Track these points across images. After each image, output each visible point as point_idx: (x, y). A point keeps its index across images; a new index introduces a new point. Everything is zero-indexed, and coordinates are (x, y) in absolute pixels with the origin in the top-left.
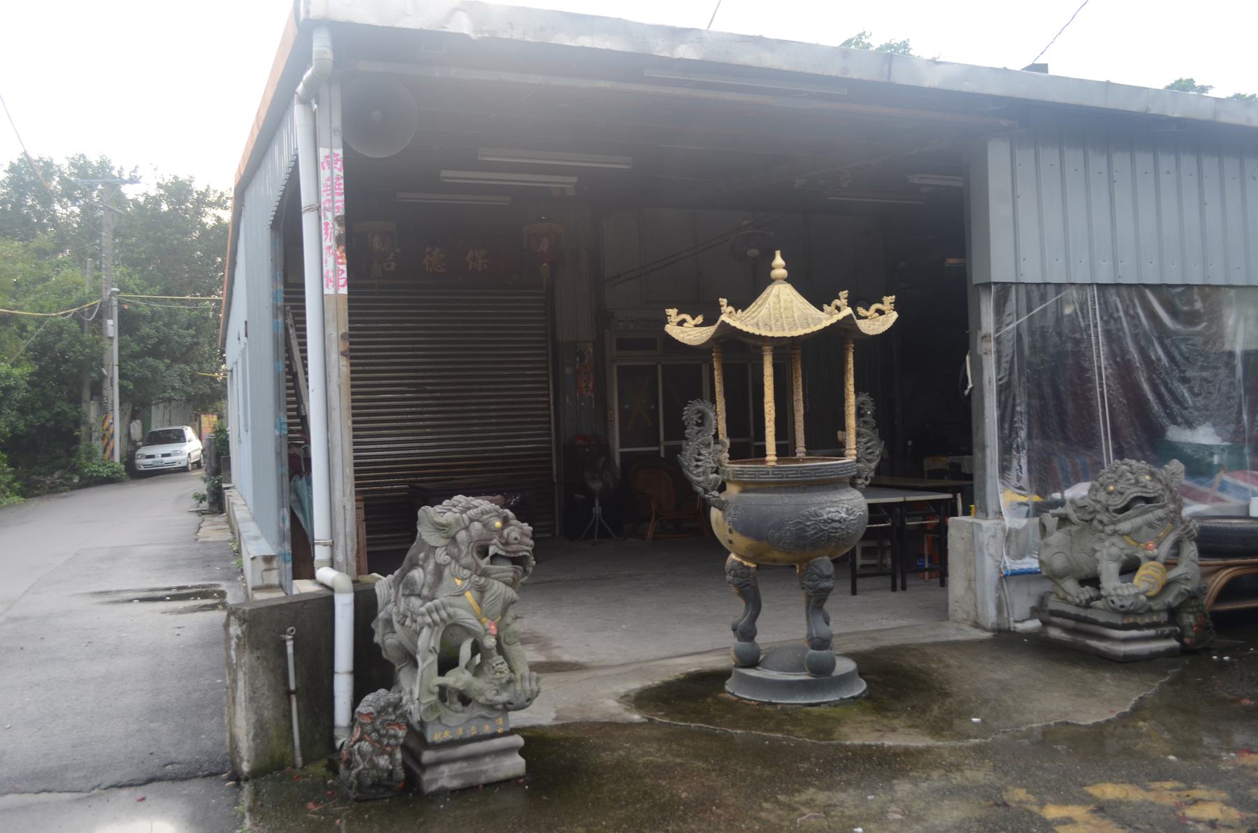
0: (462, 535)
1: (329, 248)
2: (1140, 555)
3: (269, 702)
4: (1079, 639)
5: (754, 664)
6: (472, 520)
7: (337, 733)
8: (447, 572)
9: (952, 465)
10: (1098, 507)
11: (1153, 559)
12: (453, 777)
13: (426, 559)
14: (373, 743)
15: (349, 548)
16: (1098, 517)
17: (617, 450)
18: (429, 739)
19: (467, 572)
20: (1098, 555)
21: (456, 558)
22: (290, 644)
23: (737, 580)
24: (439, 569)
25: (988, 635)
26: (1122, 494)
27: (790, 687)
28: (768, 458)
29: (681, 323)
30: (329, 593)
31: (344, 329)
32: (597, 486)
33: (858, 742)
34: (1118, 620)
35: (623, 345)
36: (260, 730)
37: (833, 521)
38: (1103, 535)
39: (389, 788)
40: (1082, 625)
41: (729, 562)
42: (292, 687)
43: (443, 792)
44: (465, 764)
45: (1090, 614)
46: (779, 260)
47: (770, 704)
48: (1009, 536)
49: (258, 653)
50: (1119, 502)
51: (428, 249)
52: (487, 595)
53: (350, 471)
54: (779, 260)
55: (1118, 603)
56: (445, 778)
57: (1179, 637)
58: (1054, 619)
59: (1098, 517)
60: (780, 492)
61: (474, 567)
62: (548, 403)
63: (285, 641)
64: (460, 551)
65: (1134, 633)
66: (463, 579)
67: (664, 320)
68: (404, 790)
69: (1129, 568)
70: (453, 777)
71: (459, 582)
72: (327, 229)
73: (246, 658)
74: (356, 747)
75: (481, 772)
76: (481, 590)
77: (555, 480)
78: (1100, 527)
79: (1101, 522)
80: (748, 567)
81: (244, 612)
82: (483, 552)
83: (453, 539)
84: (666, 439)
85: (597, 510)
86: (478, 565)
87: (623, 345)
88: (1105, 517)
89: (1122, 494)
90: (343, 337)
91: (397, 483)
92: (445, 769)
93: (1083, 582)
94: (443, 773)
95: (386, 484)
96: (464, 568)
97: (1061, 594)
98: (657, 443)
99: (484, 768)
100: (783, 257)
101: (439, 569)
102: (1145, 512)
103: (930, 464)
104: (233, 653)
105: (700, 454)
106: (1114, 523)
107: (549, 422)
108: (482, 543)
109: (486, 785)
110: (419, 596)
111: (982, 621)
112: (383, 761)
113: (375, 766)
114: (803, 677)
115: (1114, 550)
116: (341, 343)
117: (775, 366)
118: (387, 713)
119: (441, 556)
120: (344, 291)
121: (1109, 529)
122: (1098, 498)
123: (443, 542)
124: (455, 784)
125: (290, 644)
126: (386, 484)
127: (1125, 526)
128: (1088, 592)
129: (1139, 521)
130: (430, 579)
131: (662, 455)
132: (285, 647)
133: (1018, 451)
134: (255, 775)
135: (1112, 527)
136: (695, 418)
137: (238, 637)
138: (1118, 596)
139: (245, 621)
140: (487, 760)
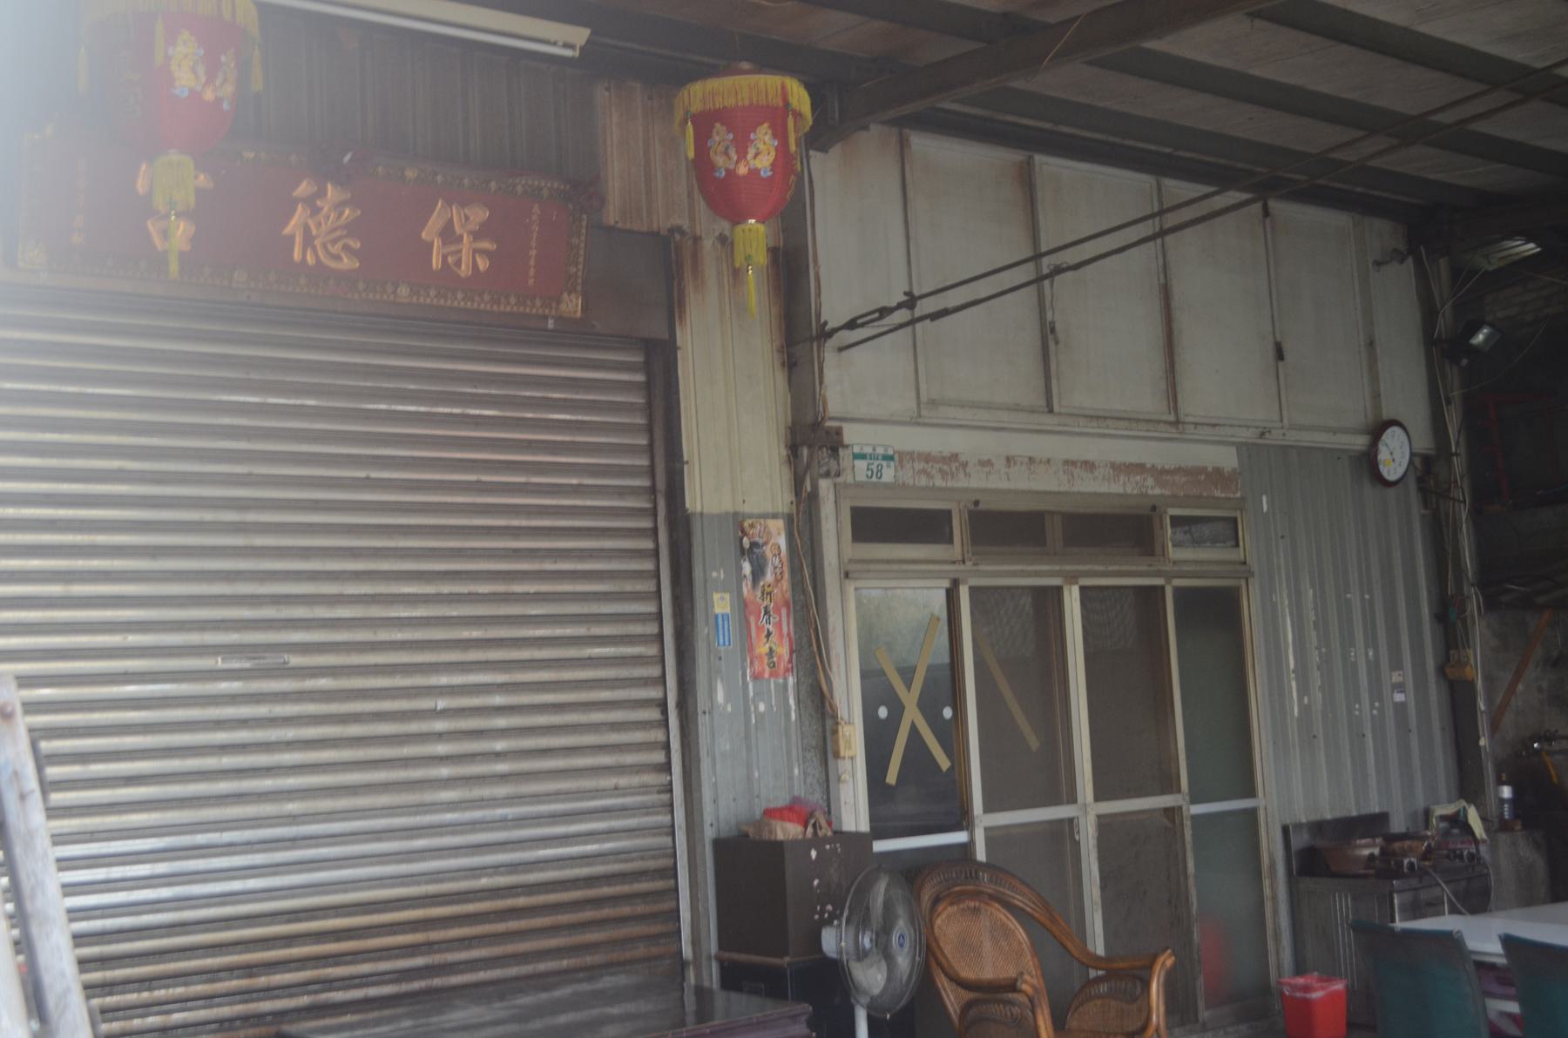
35: (874, 524)
51: (304, 188)
62: (663, 705)
77: (687, 951)
84: (989, 808)
87: (874, 524)
91: (183, 1002)
98: (961, 819)
107: (666, 767)
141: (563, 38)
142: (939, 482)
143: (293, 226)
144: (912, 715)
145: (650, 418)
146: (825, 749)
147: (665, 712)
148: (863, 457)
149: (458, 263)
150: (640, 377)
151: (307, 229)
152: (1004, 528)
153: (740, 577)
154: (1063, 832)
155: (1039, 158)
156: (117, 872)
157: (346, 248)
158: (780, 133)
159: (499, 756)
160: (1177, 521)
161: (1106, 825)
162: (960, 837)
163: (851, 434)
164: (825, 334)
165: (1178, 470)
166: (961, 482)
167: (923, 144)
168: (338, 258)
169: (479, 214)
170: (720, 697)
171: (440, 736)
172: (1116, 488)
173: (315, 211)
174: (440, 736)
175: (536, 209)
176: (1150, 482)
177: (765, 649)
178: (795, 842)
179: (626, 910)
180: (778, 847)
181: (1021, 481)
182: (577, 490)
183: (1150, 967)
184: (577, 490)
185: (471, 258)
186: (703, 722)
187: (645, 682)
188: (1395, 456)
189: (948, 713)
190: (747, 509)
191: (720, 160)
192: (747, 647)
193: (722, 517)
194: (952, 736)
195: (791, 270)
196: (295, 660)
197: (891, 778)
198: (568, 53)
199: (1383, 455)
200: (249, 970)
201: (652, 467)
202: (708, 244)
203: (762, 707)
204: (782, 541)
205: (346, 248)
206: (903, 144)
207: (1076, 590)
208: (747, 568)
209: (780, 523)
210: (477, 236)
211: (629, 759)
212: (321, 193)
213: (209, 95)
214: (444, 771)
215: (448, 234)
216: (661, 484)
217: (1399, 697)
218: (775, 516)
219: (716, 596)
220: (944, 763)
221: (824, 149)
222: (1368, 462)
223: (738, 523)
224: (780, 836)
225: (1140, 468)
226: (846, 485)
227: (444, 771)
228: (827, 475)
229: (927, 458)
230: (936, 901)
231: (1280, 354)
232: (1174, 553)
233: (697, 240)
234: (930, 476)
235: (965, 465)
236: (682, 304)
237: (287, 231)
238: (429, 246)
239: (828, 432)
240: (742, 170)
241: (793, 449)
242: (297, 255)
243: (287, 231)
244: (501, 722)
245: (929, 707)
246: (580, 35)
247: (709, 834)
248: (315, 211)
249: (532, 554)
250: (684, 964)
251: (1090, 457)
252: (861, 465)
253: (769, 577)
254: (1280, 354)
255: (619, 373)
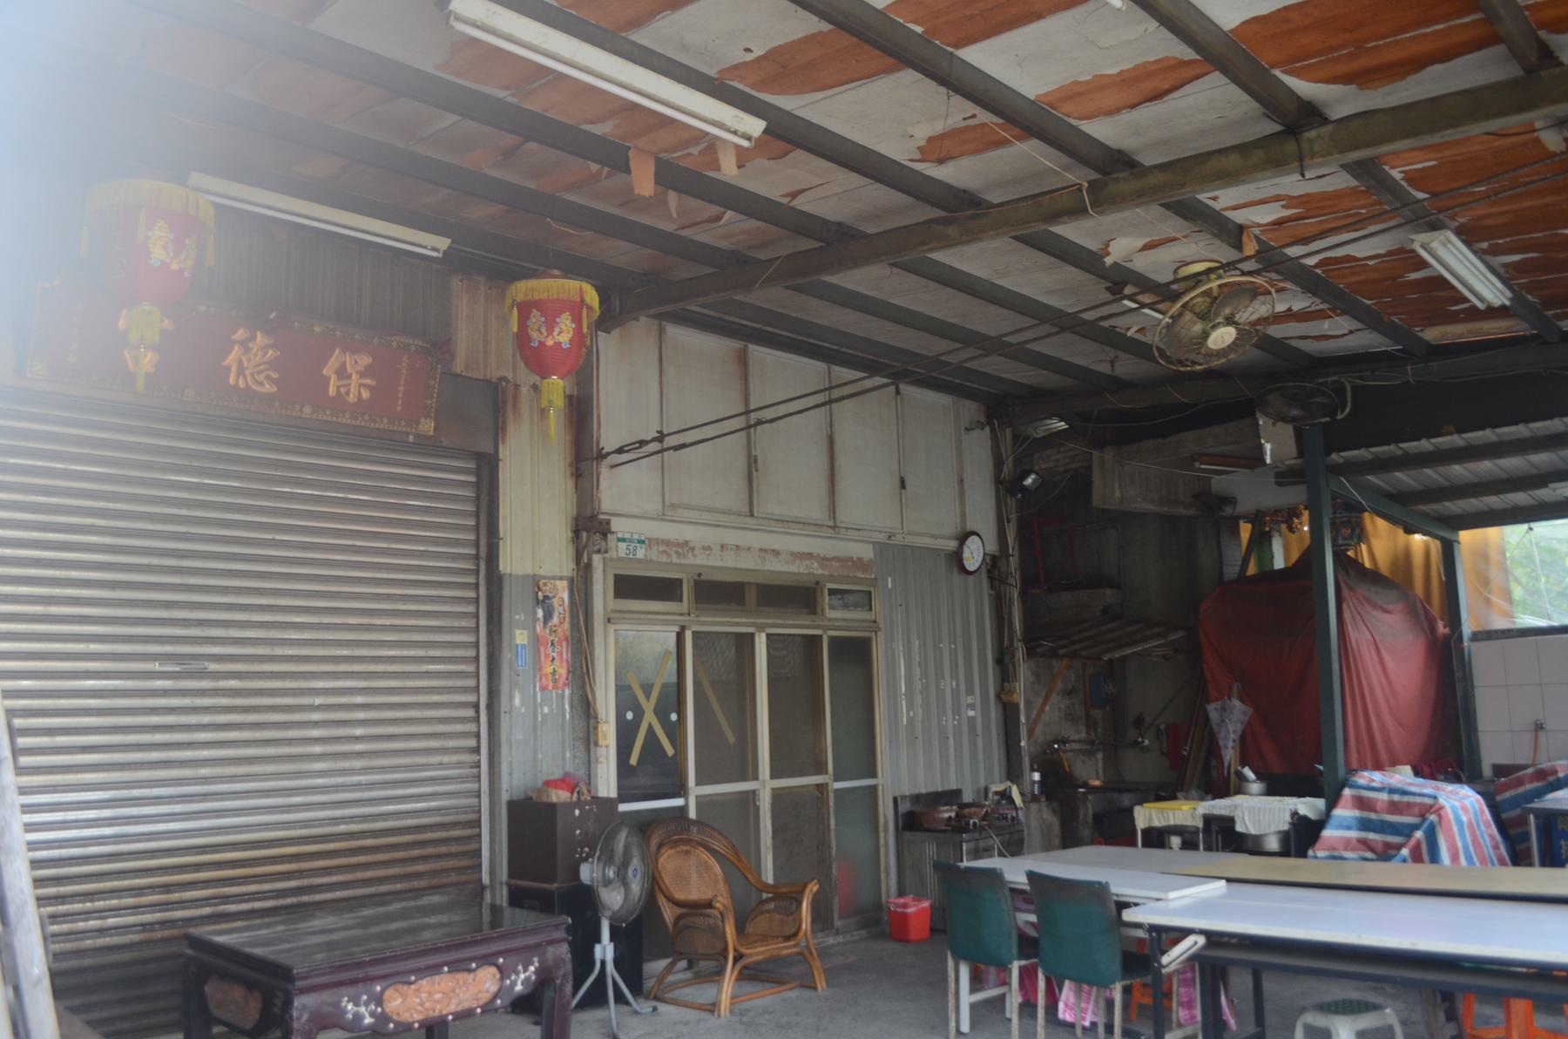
9: (1208, 820)
35: (629, 587)
51: (241, 334)
62: (476, 706)
77: (486, 879)
84: (699, 783)
87: (629, 587)
91: (116, 911)
95: (88, 915)
98: (680, 790)
103: (1147, 816)
107: (477, 750)
126: (88, 915)
141: (433, 244)
142: (675, 560)
143: (231, 360)
144: (649, 718)
145: (478, 507)
146: (589, 739)
147: (478, 711)
148: (624, 540)
149: (348, 393)
150: (472, 479)
151: (240, 363)
152: (718, 593)
153: (536, 620)
154: (749, 799)
155: (751, 347)
156: (72, 815)
157: (268, 378)
158: (577, 319)
159: (358, 739)
160: (832, 592)
161: (777, 795)
162: (678, 802)
163: (617, 525)
164: (602, 456)
165: (835, 558)
166: (690, 560)
167: (674, 332)
168: (261, 384)
169: (365, 360)
170: (517, 701)
172: (793, 569)
173: (247, 350)
174: (316, 724)
175: (405, 359)
176: (816, 565)
177: (550, 670)
178: (564, 804)
179: (444, 849)
180: (552, 808)
181: (730, 561)
182: (423, 555)
183: (802, 892)
184: (423, 555)
185: (357, 390)
186: (504, 719)
187: (465, 690)
188: (974, 555)
189: (674, 717)
190: (542, 573)
191: (534, 335)
192: (537, 666)
193: (525, 577)
194: (676, 732)
195: (580, 411)
196: (213, 667)
197: (634, 760)
198: (435, 254)
199: (966, 554)
200: (167, 888)
201: (478, 540)
202: (525, 390)
203: (546, 710)
204: (566, 596)
205: (268, 378)
206: (661, 332)
207: (763, 636)
208: (540, 613)
209: (565, 583)
210: (362, 374)
211: (451, 743)
212: (253, 338)
213: (175, 266)
214: (318, 749)
215: (342, 373)
216: (483, 554)
217: (971, 713)
218: (561, 578)
219: (518, 632)
220: (670, 751)
221: (608, 331)
222: (956, 558)
223: (535, 582)
224: (554, 799)
225: (809, 556)
226: (611, 559)
227: (318, 749)
228: (599, 551)
229: (667, 543)
230: (661, 845)
231: (903, 485)
232: (830, 614)
233: (517, 387)
234: (669, 555)
235: (693, 549)
236: (504, 429)
237: (226, 363)
238: (329, 379)
239: (601, 523)
240: (550, 342)
241: (576, 533)
242: (232, 381)
243: (226, 363)
244: (361, 715)
245: (661, 714)
246: (443, 243)
247: (505, 797)
248: (247, 350)
249: (389, 597)
250: (483, 888)
251: (776, 547)
252: (622, 545)
253: (555, 620)
254: (903, 485)
255: (458, 476)
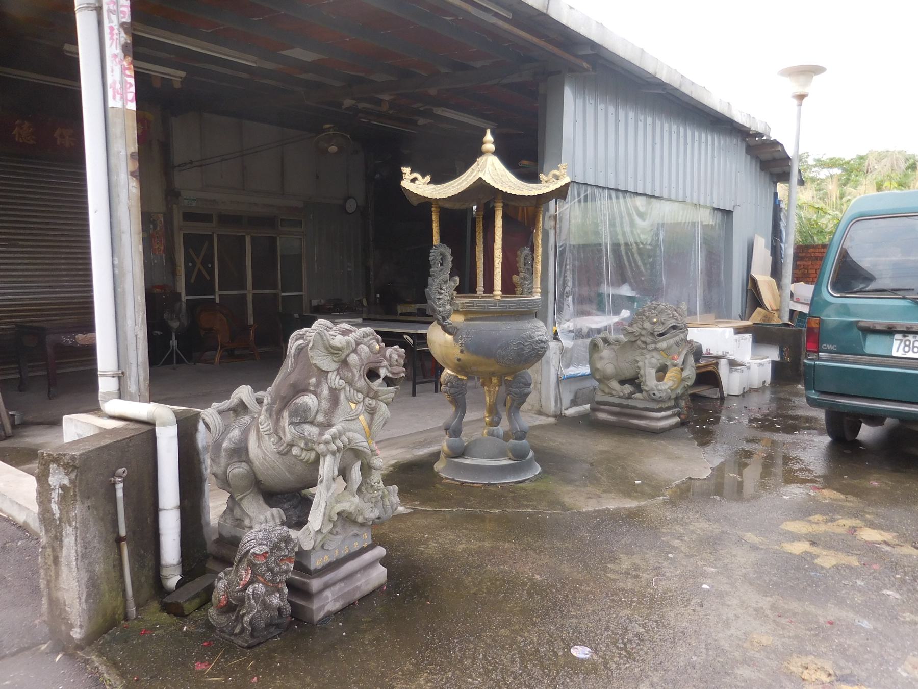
0: (353, 359)
1: (115, 56)
2: (668, 363)
3: (100, 555)
4: (623, 419)
5: (462, 455)
6: (358, 344)
7: (165, 572)
8: (342, 397)
9: (419, 310)
10: (644, 332)
11: (675, 366)
12: (336, 600)
13: (318, 384)
14: (265, 584)
15: (141, 378)
16: (643, 339)
17: (184, 297)
18: (312, 568)
19: (360, 396)
20: (640, 364)
21: (350, 383)
22: (120, 488)
23: (452, 390)
24: (334, 395)
25: (552, 420)
26: (663, 323)
27: (502, 470)
28: (495, 293)
29: (414, 180)
30: (146, 428)
31: (134, 147)
32: (175, 324)
33: (590, 509)
34: (656, 406)
35: (188, 217)
36: (93, 587)
37: (542, 342)
38: (644, 351)
39: (278, 626)
40: (625, 411)
41: (444, 374)
42: (123, 532)
43: (330, 616)
44: (342, 585)
45: (631, 402)
46: (489, 137)
47: (489, 484)
48: (563, 351)
49: (88, 503)
50: (660, 329)
52: (376, 417)
53: (141, 299)
54: (489, 137)
55: (658, 395)
56: (327, 602)
57: (679, 415)
58: (602, 407)
59: (643, 339)
60: (501, 320)
61: (365, 391)
63: (114, 484)
64: (353, 374)
65: (663, 414)
66: (357, 403)
67: (400, 176)
68: (294, 626)
69: (662, 370)
70: (336, 600)
71: (353, 406)
72: (111, 33)
73: (78, 510)
74: (250, 590)
75: (358, 588)
76: (372, 412)
78: (644, 346)
79: (644, 343)
80: (462, 380)
81: (73, 458)
82: (372, 374)
83: (345, 363)
84: (220, 289)
85: (174, 343)
86: (369, 387)
88: (649, 339)
89: (663, 323)
90: (132, 155)
92: (328, 593)
93: (622, 382)
94: (327, 597)
96: (358, 391)
97: (607, 390)
98: (213, 293)
99: (358, 584)
100: (493, 133)
101: (334, 395)
102: (676, 336)
103: (401, 309)
104: (54, 507)
105: (441, 289)
106: (655, 343)
108: (372, 366)
109: (362, 599)
110: (312, 423)
111: (544, 410)
112: (275, 600)
113: (266, 606)
114: (505, 462)
115: (654, 361)
116: (130, 161)
117: (504, 217)
118: (280, 549)
119: (335, 380)
120: (132, 106)
121: (651, 347)
122: (645, 326)
123: (334, 366)
124: (337, 606)
125: (120, 488)
127: (663, 345)
128: (628, 389)
129: (672, 341)
130: (325, 405)
131: (217, 301)
132: (115, 490)
133: (567, 296)
134: (90, 640)
135: (653, 346)
136: (439, 258)
137: (63, 487)
138: (659, 390)
139: (75, 467)
140: (359, 575)
144: (199, 266)
146: (174, 273)
152: (227, 219)
161: (254, 295)
171: (63, 264)
188: (351, 206)
194: (211, 272)
196: (21, 243)
197: (192, 281)
199: (348, 205)
220: (208, 278)
222: (343, 208)
231: (317, 177)
254: (317, 177)
